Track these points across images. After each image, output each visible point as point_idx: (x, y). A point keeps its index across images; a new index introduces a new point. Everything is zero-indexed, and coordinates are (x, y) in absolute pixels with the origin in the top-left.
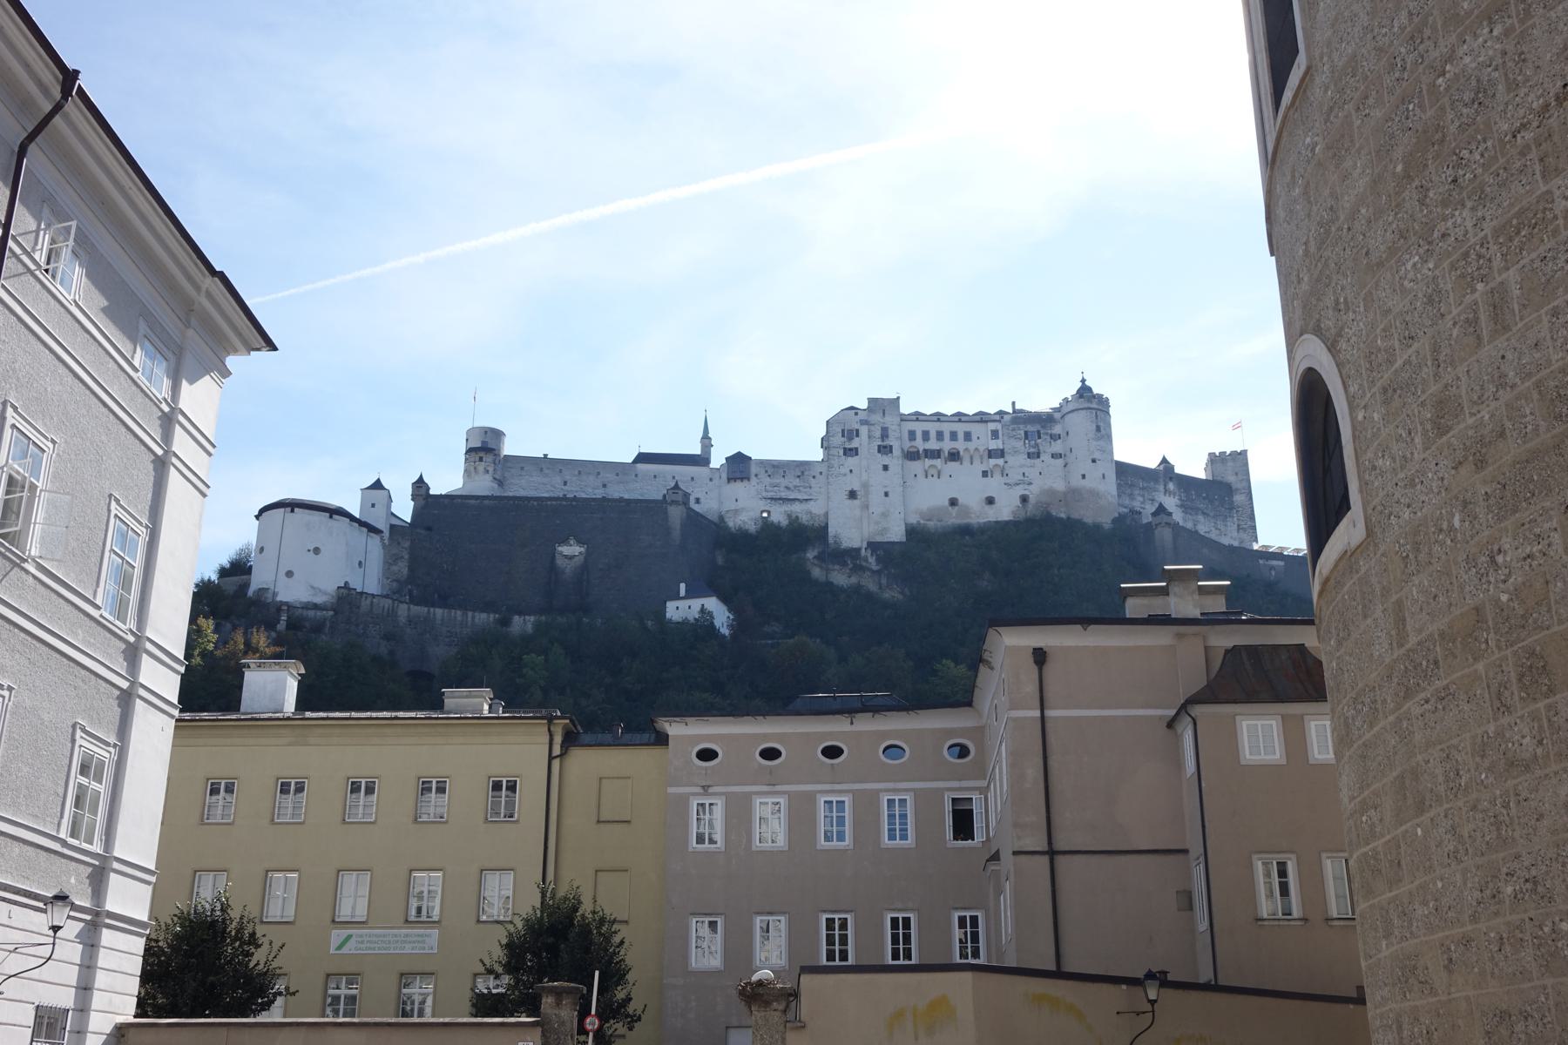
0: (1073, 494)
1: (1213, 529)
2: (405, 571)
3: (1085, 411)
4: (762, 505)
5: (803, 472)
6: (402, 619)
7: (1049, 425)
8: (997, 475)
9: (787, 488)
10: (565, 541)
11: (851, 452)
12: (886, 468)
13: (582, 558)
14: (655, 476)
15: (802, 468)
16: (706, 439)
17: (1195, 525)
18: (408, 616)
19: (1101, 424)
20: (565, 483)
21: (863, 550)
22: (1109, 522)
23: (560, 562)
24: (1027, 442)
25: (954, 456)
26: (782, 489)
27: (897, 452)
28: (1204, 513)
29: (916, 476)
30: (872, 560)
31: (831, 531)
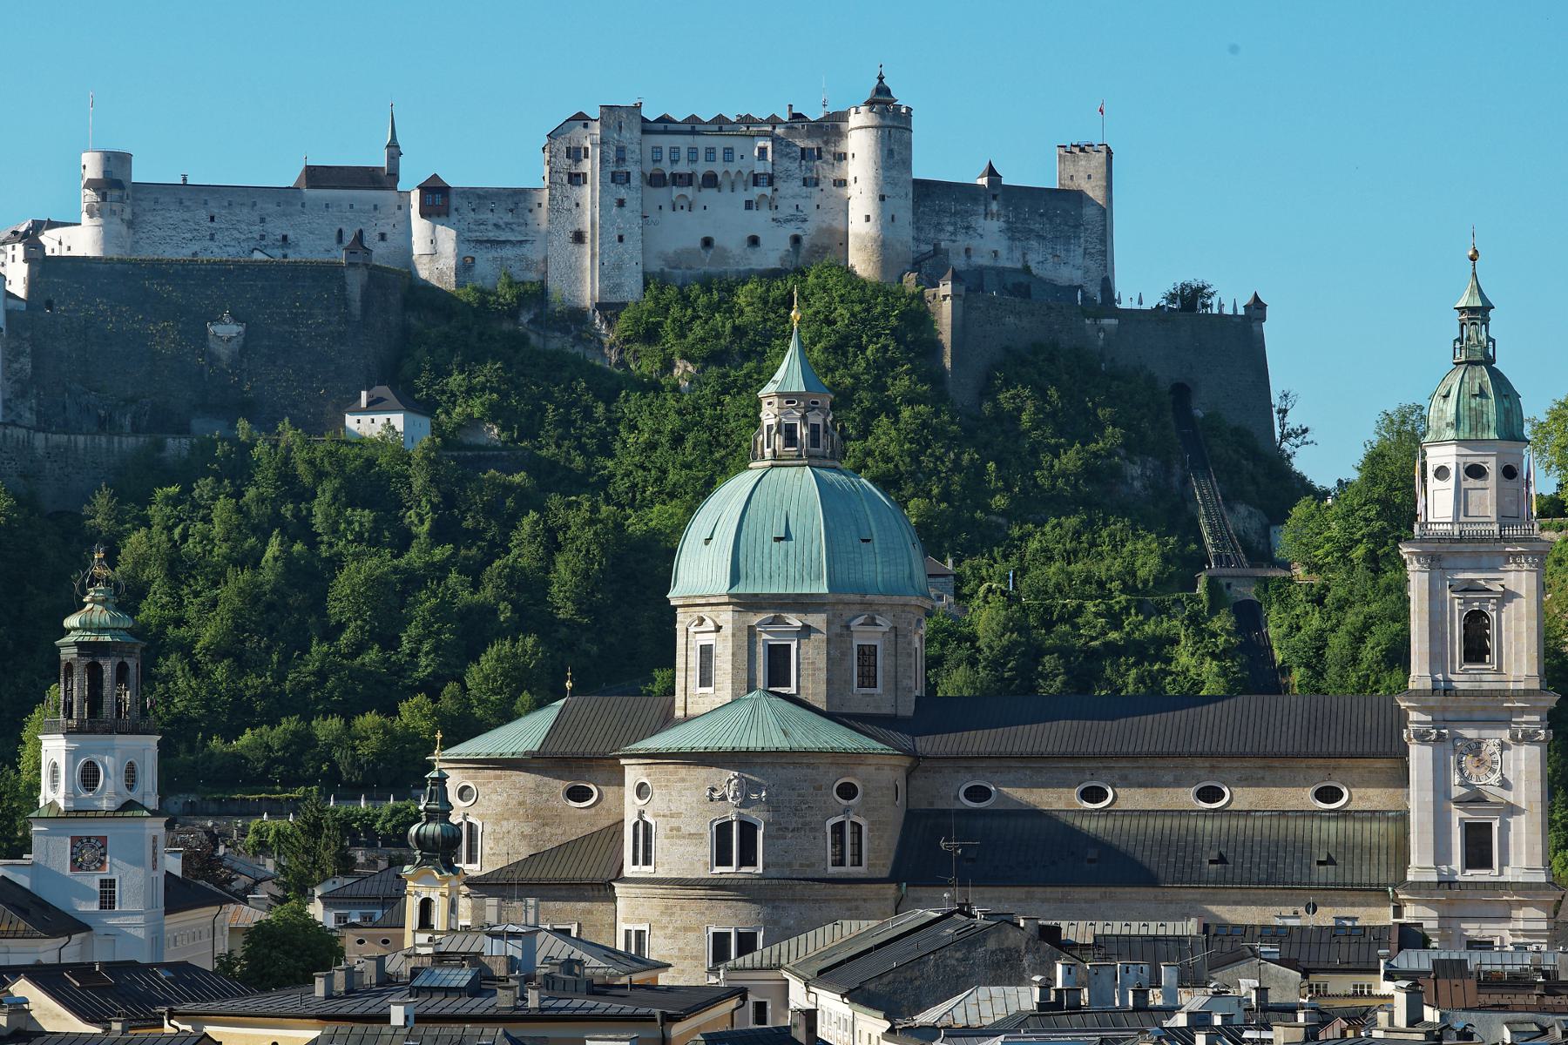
1: (1050, 257)
2: (29, 368)
6: (40, 452)
9: (496, 226)
10: (220, 321)
11: (576, 179)
12: (621, 203)
13: (240, 339)
14: (327, 206)
16: (394, 149)
17: (1024, 255)
18: (46, 447)
20: (212, 219)
23: (213, 345)
24: (803, 162)
25: (711, 181)
26: (490, 228)
28: (1040, 237)
29: (660, 207)
31: (553, 285)
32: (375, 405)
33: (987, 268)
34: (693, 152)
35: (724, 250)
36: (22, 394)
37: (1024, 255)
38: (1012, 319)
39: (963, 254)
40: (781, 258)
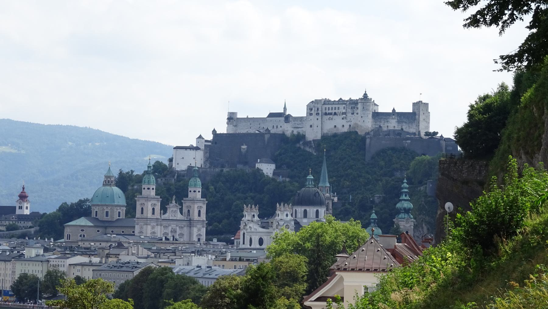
2: (208, 155)
4: (292, 129)
8: (345, 119)
9: (298, 124)
10: (243, 145)
11: (311, 114)
12: (317, 119)
15: (301, 119)
16: (285, 109)
17: (402, 127)
19: (365, 107)
21: (312, 142)
22: (364, 133)
23: (242, 150)
25: (335, 114)
27: (320, 115)
28: (405, 123)
30: (313, 144)
32: (260, 162)
33: (392, 130)
34: (332, 108)
36: (207, 161)
37: (402, 127)
38: (384, 141)
39: (386, 127)
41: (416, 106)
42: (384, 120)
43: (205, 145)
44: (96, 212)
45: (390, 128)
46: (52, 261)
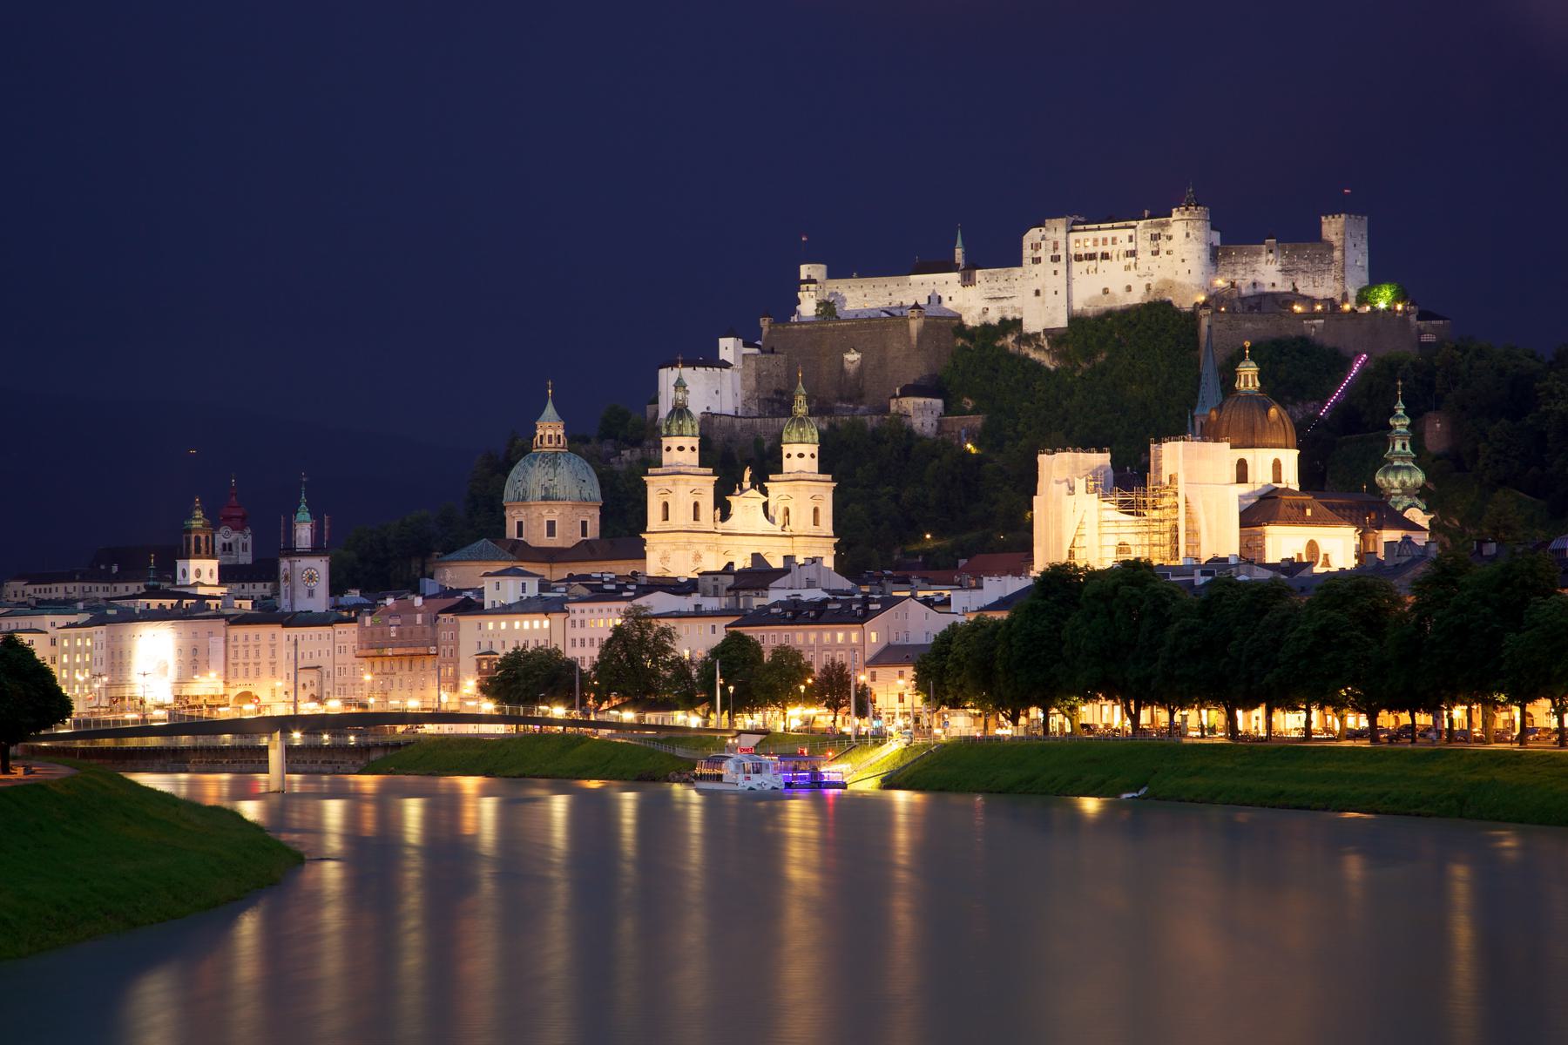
0: (1169, 285)
2: (754, 383)
3: (1180, 222)
4: (985, 304)
5: (1009, 276)
7: (1166, 228)
9: (999, 289)
10: (848, 351)
11: (1037, 261)
12: (1055, 273)
13: (859, 362)
17: (1294, 284)
23: (846, 365)
25: (1105, 256)
27: (1063, 259)
28: (1304, 272)
30: (1046, 342)
35: (1114, 294)
37: (1294, 284)
40: (1142, 298)
41: (1333, 226)
42: (1244, 267)
43: (744, 355)
44: (520, 524)
45: (1259, 289)
46: (578, 612)
